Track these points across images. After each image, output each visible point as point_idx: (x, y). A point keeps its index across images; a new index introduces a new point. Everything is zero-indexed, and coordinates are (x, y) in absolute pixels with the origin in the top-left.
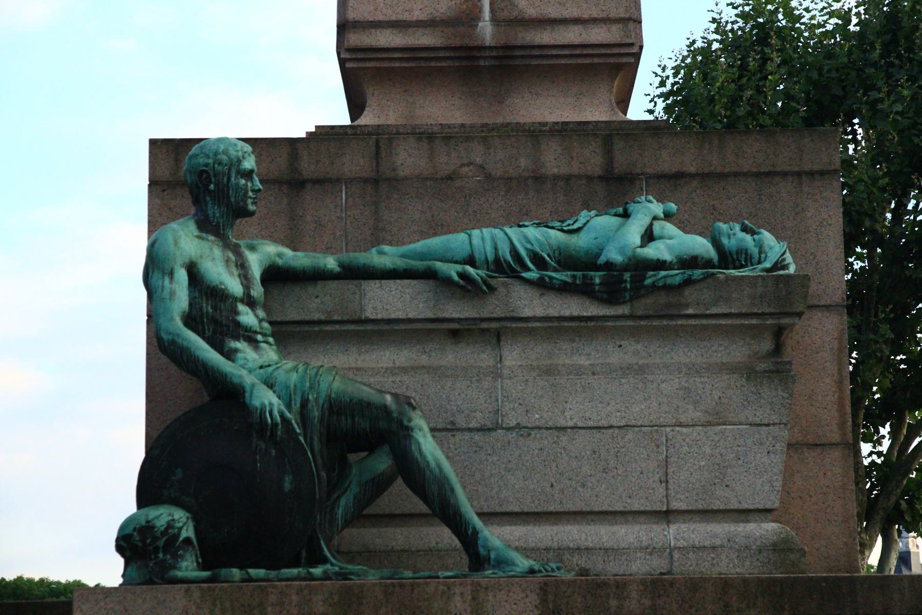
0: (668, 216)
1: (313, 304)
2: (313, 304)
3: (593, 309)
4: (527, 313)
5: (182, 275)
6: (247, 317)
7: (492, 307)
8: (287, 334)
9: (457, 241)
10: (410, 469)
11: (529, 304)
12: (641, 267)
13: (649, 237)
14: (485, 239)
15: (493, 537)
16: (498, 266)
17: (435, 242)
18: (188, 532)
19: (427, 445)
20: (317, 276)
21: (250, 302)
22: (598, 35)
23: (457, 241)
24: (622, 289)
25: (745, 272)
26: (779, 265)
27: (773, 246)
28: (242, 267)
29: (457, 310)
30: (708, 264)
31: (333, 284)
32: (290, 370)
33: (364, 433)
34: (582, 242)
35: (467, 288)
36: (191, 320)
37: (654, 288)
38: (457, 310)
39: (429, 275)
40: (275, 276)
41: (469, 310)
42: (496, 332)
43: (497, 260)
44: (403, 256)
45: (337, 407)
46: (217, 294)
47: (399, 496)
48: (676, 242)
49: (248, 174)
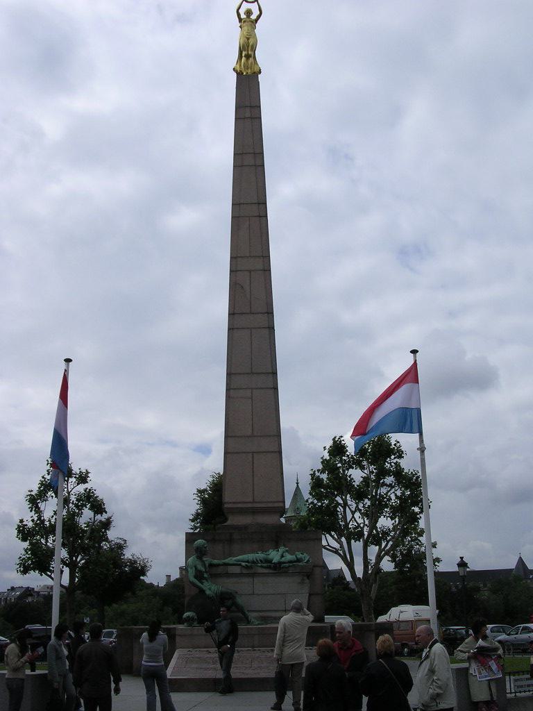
0: (287, 551)
1: (220, 570)
2: (220, 570)
3: (271, 571)
4: (259, 572)
5: (194, 569)
6: (206, 575)
7: (252, 571)
8: (214, 576)
9: (245, 557)
10: (235, 604)
11: (261, 570)
12: (280, 563)
13: (282, 556)
14: (250, 557)
15: (252, 615)
16: (253, 562)
17: (240, 557)
18: (196, 617)
19: (239, 600)
20: (218, 565)
21: (206, 572)
22: (276, 505)
23: (245, 557)
24: (278, 569)
25: (300, 564)
26: (308, 561)
27: (306, 557)
28: (205, 565)
29: (245, 571)
30: (295, 562)
31: (222, 567)
32: (214, 587)
33: (226, 598)
34: (270, 557)
35: (247, 567)
36: (196, 577)
37: (283, 568)
38: (245, 571)
39: (240, 565)
40: (211, 565)
41: (250, 570)
42: (253, 575)
43: (253, 561)
44: (235, 561)
45: (222, 593)
46: (200, 571)
47: (234, 608)
48: (289, 557)
49: (205, 548)
